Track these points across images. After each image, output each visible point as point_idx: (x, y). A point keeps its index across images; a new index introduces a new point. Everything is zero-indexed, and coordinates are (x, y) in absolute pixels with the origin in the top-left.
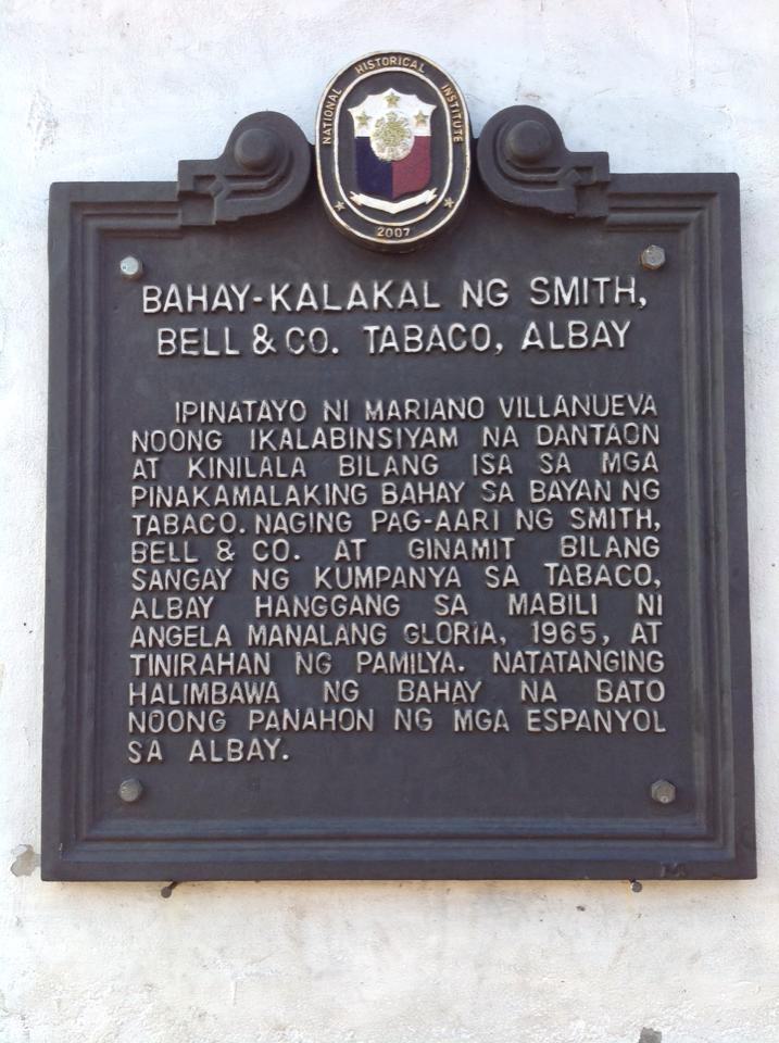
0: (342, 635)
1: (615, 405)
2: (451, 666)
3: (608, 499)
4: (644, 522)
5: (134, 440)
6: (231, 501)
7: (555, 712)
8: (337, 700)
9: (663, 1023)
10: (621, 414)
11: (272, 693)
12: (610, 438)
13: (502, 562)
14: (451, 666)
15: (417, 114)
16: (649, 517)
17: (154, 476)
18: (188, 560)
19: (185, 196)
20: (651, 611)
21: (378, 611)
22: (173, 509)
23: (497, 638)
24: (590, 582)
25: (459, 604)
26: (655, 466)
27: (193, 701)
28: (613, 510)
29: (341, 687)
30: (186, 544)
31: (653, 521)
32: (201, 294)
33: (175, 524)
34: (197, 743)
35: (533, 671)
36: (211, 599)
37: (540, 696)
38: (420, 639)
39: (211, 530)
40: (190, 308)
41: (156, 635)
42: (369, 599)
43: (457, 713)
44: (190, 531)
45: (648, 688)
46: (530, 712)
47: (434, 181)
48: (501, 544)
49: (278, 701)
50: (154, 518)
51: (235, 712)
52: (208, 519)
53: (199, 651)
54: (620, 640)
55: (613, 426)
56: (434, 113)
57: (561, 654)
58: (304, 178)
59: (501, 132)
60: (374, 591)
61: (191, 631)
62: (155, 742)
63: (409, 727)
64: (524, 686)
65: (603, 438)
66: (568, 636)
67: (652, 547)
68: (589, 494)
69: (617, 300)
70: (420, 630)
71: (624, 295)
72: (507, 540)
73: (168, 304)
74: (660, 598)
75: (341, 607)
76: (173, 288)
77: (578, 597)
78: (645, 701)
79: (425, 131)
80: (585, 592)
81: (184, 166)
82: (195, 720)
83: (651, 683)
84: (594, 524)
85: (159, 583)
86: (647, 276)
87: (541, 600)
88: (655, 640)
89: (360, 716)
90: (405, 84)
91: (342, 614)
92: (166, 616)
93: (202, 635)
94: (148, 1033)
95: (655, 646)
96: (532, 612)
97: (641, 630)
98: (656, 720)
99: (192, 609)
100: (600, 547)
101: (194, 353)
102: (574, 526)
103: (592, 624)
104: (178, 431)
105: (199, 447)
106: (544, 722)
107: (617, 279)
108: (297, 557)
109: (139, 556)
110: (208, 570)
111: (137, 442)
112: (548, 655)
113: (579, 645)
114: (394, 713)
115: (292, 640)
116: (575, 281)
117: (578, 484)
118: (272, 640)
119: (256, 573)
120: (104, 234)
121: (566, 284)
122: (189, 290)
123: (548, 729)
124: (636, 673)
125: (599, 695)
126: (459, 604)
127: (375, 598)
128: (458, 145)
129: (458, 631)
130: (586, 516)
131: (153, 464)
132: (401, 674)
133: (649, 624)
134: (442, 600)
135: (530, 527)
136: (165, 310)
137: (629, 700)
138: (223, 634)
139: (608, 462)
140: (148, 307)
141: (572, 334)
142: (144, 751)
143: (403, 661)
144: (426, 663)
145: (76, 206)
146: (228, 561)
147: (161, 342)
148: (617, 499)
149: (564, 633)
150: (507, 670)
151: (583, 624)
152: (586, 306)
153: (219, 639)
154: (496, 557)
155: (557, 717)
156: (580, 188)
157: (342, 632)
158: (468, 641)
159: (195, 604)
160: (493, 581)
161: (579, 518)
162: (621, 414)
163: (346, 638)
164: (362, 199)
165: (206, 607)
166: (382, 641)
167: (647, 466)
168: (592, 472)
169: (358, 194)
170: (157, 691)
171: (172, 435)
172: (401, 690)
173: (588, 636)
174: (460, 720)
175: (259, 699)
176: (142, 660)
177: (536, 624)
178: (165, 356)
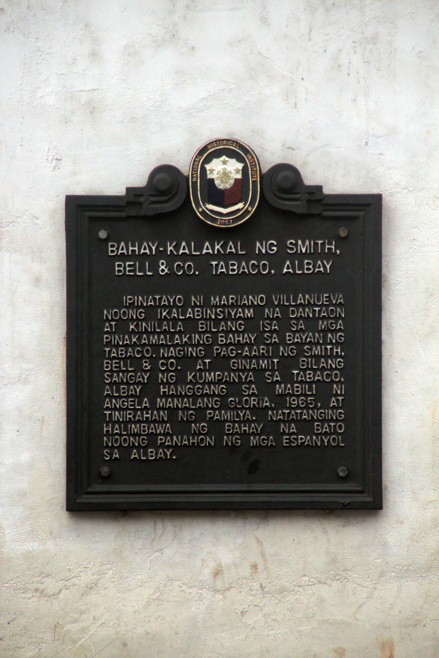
0: (200, 403)
1: (325, 299)
2: (249, 417)
3: (321, 342)
4: (337, 352)
5: (105, 314)
6: (149, 342)
7: (296, 437)
8: (197, 432)
9: (343, 578)
10: (328, 303)
11: (168, 429)
12: (322, 314)
13: (273, 370)
14: (249, 417)
15: (236, 168)
16: (339, 350)
17: (114, 330)
18: (130, 369)
19: (129, 203)
20: (339, 392)
21: (216, 392)
22: (122, 346)
23: (270, 405)
24: (312, 380)
25: (253, 389)
26: (342, 327)
27: (132, 433)
28: (323, 347)
29: (199, 426)
30: (129, 361)
31: (341, 352)
32: (135, 247)
33: (123, 352)
34: (135, 451)
35: (286, 419)
36: (140, 387)
37: (289, 430)
38: (236, 406)
39: (140, 356)
40: (130, 253)
41: (116, 403)
42: (212, 387)
43: (252, 438)
44: (130, 356)
45: (337, 427)
46: (285, 437)
47: (243, 199)
48: (273, 362)
49: (171, 433)
50: (114, 350)
51: (152, 437)
52: (138, 350)
53: (135, 410)
54: (326, 406)
55: (324, 308)
56: (244, 168)
57: (299, 411)
58: (184, 196)
59: (273, 178)
60: (214, 384)
61: (131, 401)
62: (116, 450)
63: (230, 444)
64: (282, 426)
65: (320, 313)
66: (302, 404)
67: (340, 364)
68: (312, 340)
69: (326, 251)
70: (235, 401)
71: (330, 249)
72: (275, 361)
73: (120, 251)
74: (343, 386)
75: (199, 390)
76: (122, 244)
77: (307, 386)
78: (335, 432)
79: (239, 176)
80: (310, 383)
81: (128, 189)
82: (134, 441)
83: (338, 424)
84: (315, 353)
85: (116, 379)
86: (340, 241)
87: (290, 388)
88: (340, 405)
89: (208, 439)
90: (231, 154)
91: (200, 394)
92: (120, 394)
93: (136, 403)
94: (110, 583)
95: (341, 408)
96: (286, 393)
97: (335, 401)
98: (340, 441)
99: (132, 391)
100: (317, 363)
101: (132, 274)
102: (306, 354)
103: (313, 398)
104: (125, 310)
105: (135, 317)
106: (291, 442)
107: (327, 241)
108: (179, 368)
109: (107, 367)
110: (139, 374)
111: (106, 315)
112: (293, 412)
113: (307, 408)
114: (224, 438)
115: (177, 405)
116: (307, 243)
117: (308, 334)
118: (168, 405)
119: (160, 375)
120: (92, 219)
121: (304, 244)
122: (130, 245)
123: (292, 444)
124: (332, 420)
125: (315, 430)
126: (253, 389)
127: (215, 387)
128: (254, 183)
129: (253, 401)
130: (311, 350)
131: (113, 325)
132: (227, 421)
133: (338, 398)
134: (245, 387)
135: (286, 355)
136: (119, 254)
137: (329, 432)
138: (146, 402)
139: (322, 325)
140: (111, 253)
141: (306, 267)
142: (111, 454)
143: (228, 415)
144: (238, 416)
145: (79, 206)
146: (148, 370)
147: (117, 269)
148: (325, 343)
149: (300, 402)
150: (274, 419)
151: (309, 398)
152: (313, 253)
153: (144, 405)
154: (270, 368)
155: (297, 439)
156: (309, 201)
157: (200, 402)
158: (257, 406)
159: (133, 389)
160: (269, 379)
161: (308, 351)
162: (328, 303)
163: (201, 405)
164: (211, 207)
165: (138, 390)
166: (218, 406)
167: (339, 327)
168: (315, 330)
169: (209, 205)
170: (117, 428)
171: (122, 312)
172: (227, 428)
173: (311, 404)
174: (253, 441)
175: (162, 432)
176: (109, 414)
177: (288, 399)
178: (118, 275)
